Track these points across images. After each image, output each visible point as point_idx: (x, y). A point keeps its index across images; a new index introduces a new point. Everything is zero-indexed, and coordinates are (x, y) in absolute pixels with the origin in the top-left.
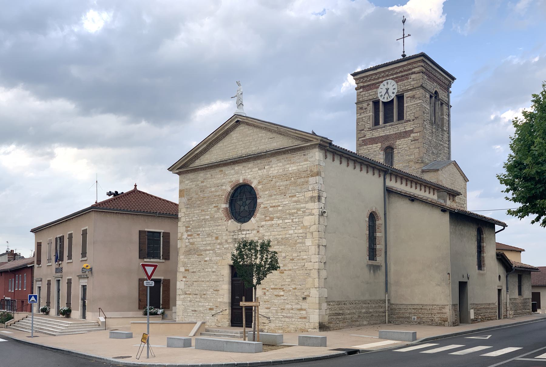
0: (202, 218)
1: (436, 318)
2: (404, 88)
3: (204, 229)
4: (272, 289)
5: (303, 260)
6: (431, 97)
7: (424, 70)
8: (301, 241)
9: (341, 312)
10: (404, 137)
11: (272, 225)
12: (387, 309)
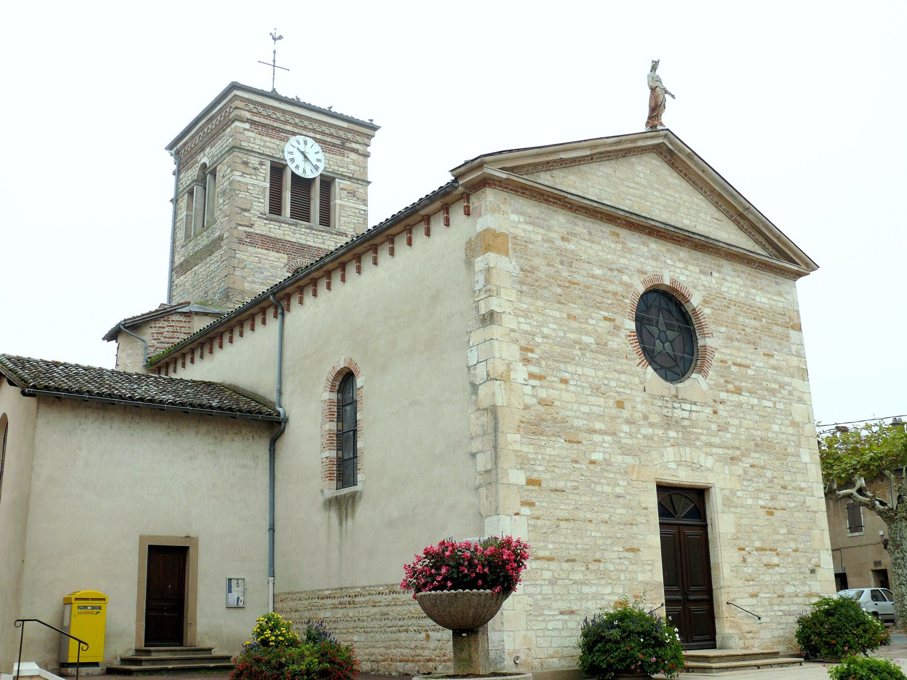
0: (572, 336)
2: (336, 168)
4: (757, 549)
11: (740, 405)
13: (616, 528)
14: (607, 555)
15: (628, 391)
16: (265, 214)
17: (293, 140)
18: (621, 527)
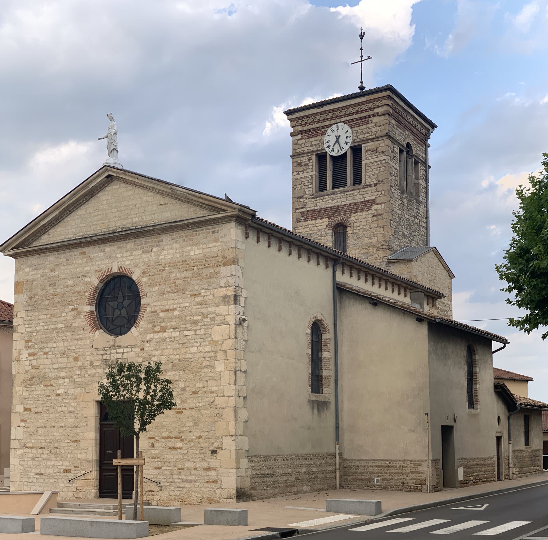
0: (52, 327)
1: (410, 480)
3: (55, 345)
4: (164, 438)
5: (212, 392)
6: (401, 151)
7: (391, 111)
8: (208, 363)
9: (269, 472)
10: (362, 210)
11: (164, 340)
12: (337, 467)
13: (68, 430)
14: (61, 444)
15: (82, 350)
16: (313, 195)
17: (329, 131)
18: (70, 429)
